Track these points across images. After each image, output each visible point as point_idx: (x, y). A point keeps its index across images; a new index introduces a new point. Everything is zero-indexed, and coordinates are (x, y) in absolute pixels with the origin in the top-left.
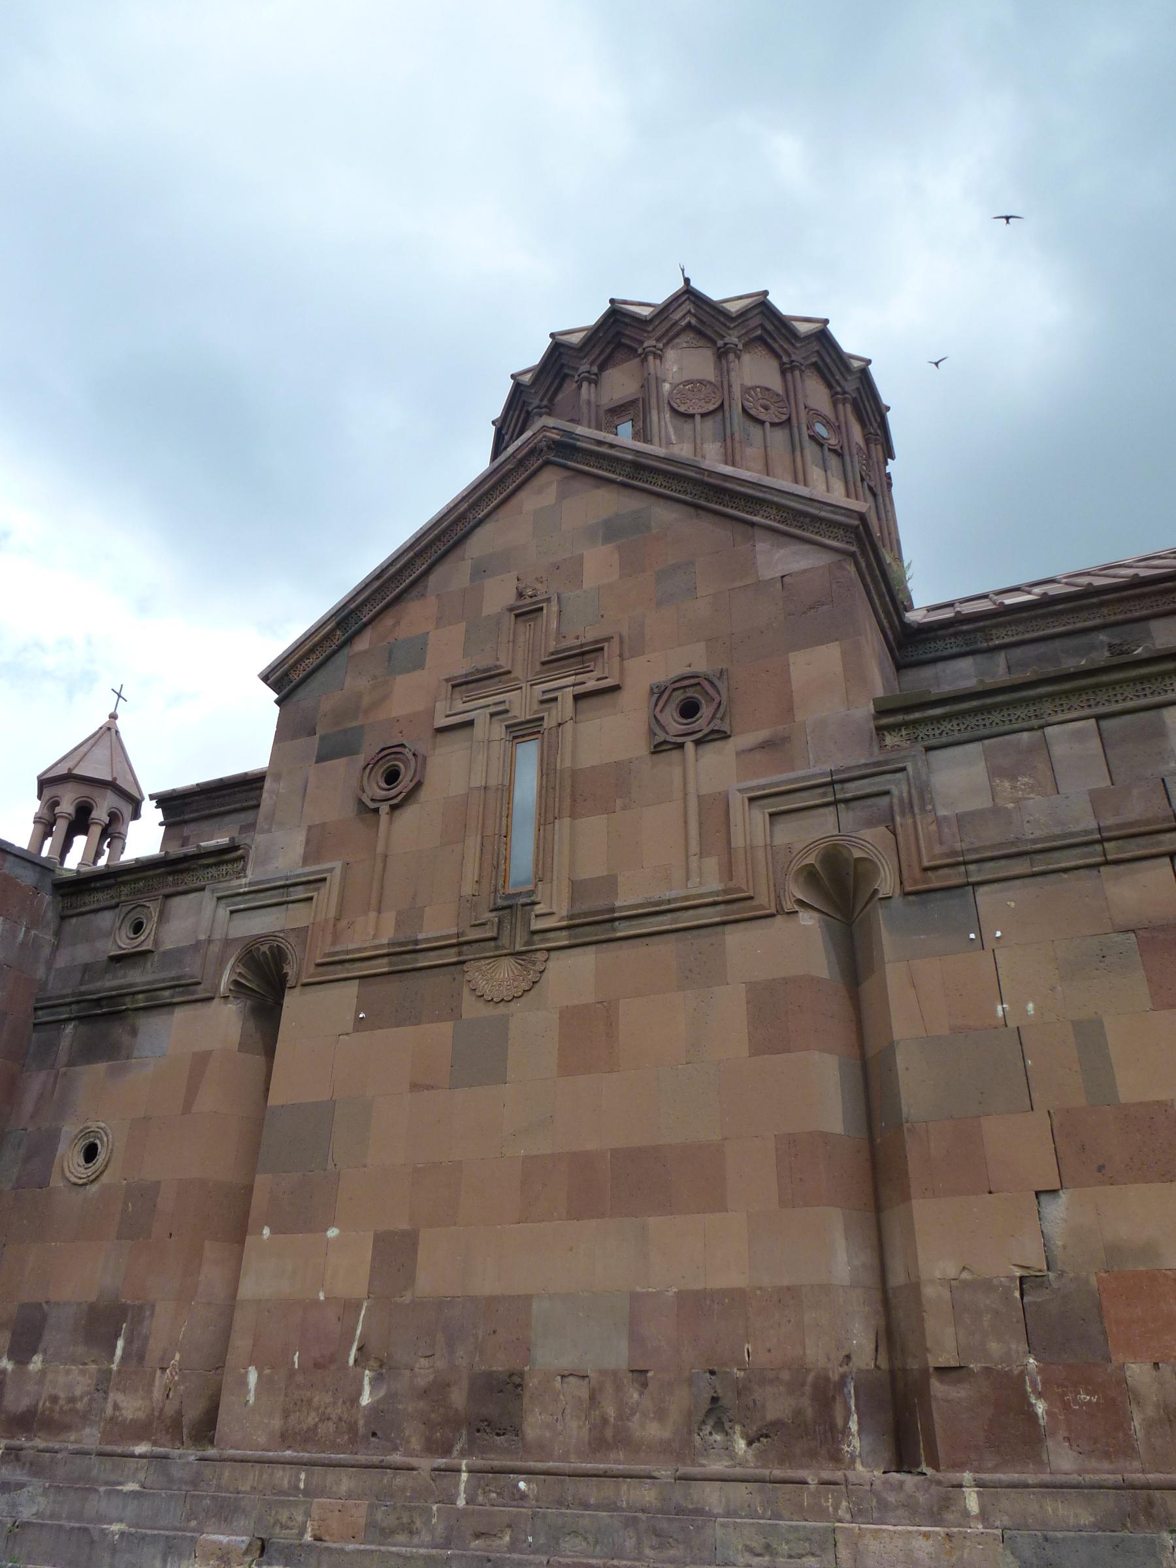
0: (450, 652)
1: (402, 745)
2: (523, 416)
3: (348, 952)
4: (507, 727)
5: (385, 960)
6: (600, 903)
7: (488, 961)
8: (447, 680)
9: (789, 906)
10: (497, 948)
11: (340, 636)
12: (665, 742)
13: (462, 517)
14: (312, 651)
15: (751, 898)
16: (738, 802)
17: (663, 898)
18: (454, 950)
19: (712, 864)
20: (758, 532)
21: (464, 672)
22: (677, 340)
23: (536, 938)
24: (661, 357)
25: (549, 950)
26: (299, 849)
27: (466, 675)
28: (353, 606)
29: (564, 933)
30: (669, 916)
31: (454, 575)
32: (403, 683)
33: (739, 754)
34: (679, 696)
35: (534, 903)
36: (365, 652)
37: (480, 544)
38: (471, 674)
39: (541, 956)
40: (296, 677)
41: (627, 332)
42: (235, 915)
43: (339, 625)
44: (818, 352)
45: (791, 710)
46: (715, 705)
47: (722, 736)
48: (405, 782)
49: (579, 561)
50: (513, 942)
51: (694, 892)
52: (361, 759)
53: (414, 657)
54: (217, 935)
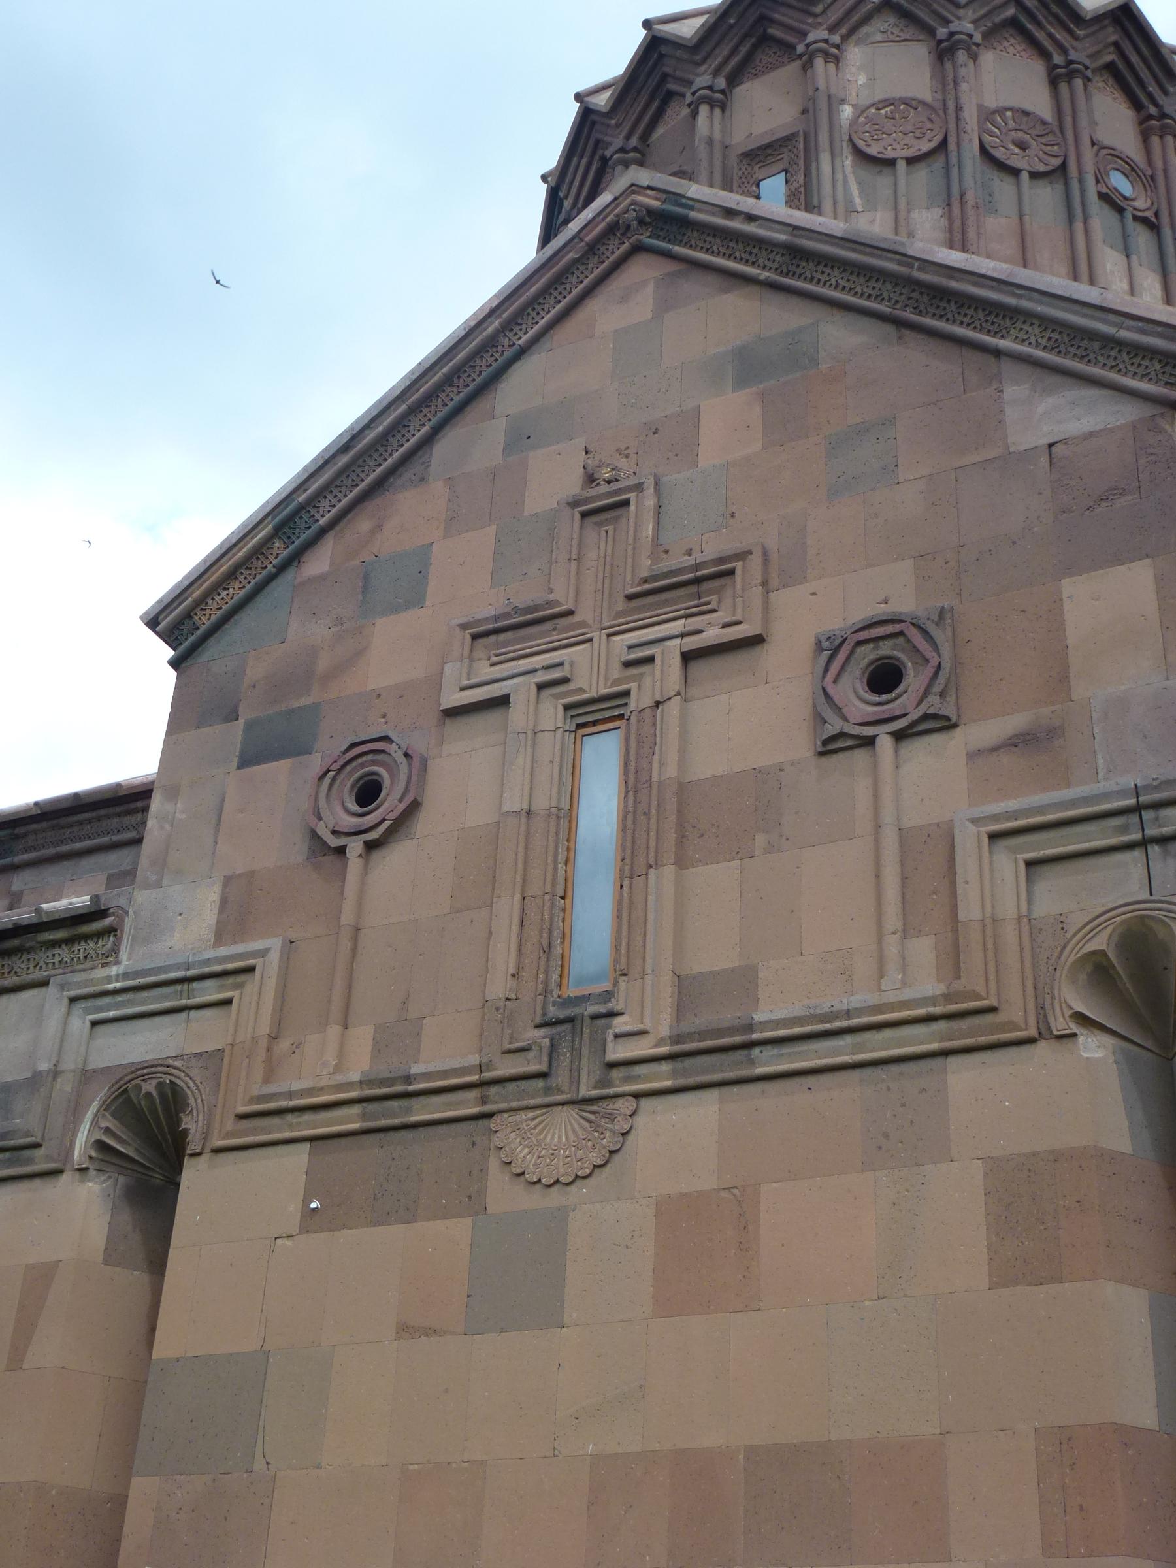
0: (468, 578)
1: (386, 739)
3: (290, 1095)
4: (567, 708)
5: (355, 1110)
6: (728, 1016)
7: (531, 1114)
8: (464, 627)
9: (1060, 1024)
10: (548, 1091)
11: (280, 551)
12: (842, 735)
13: (491, 343)
14: (232, 575)
15: (993, 1010)
16: (969, 840)
17: (838, 1007)
18: (473, 1094)
19: (923, 950)
20: (1007, 366)
21: (492, 612)
22: (865, 29)
23: (616, 1074)
24: (837, 60)
25: (637, 1096)
26: (209, 917)
27: (496, 618)
28: (302, 498)
29: (665, 1067)
30: (849, 1040)
31: (477, 443)
33: (973, 756)
34: (867, 655)
35: (612, 1014)
36: (322, 578)
37: (521, 390)
38: (506, 615)
39: (624, 1106)
40: (205, 620)
41: (777, 16)
42: (101, 1029)
43: (277, 530)
44: (1116, 44)
45: (1064, 679)
46: (929, 671)
48: (389, 804)
49: (693, 418)
50: (575, 1081)
51: (891, 997)
52: (315, 763)
53: (407, 584)
54: (70, 1063)
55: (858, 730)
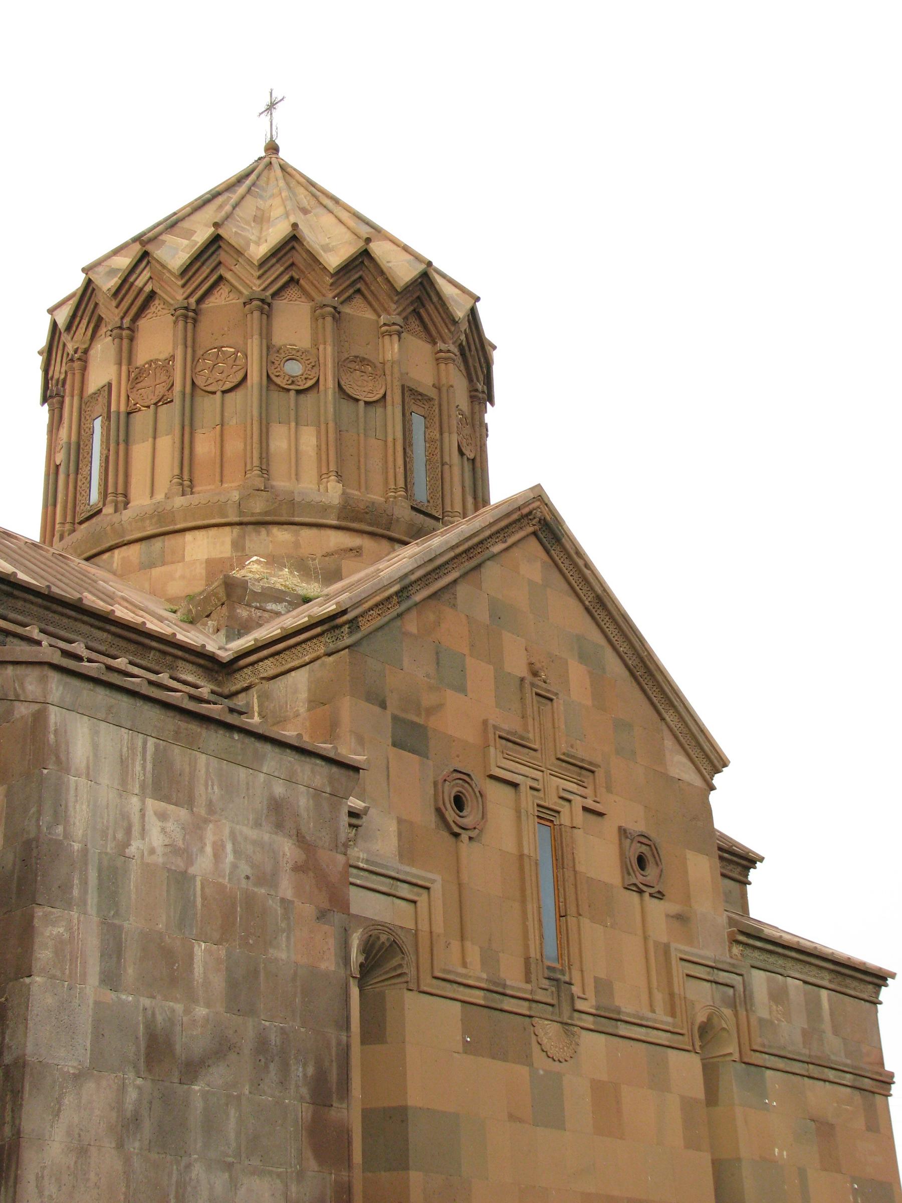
1: (468, 775)
2: (286, 278)
4: (538, 805)
7: (546, 1022)
8: (495, 727)
12: (635, 885)
16: (674, 956)
18: (526, 1004)
23: (576, 1015)
29: (591, 1018)
30: (643, 1030)
32: (452, 698)
35: (570, 984)
47: (659, 895)
48: (470, 818)
50: (560, 1014)
55: (641, 886)
